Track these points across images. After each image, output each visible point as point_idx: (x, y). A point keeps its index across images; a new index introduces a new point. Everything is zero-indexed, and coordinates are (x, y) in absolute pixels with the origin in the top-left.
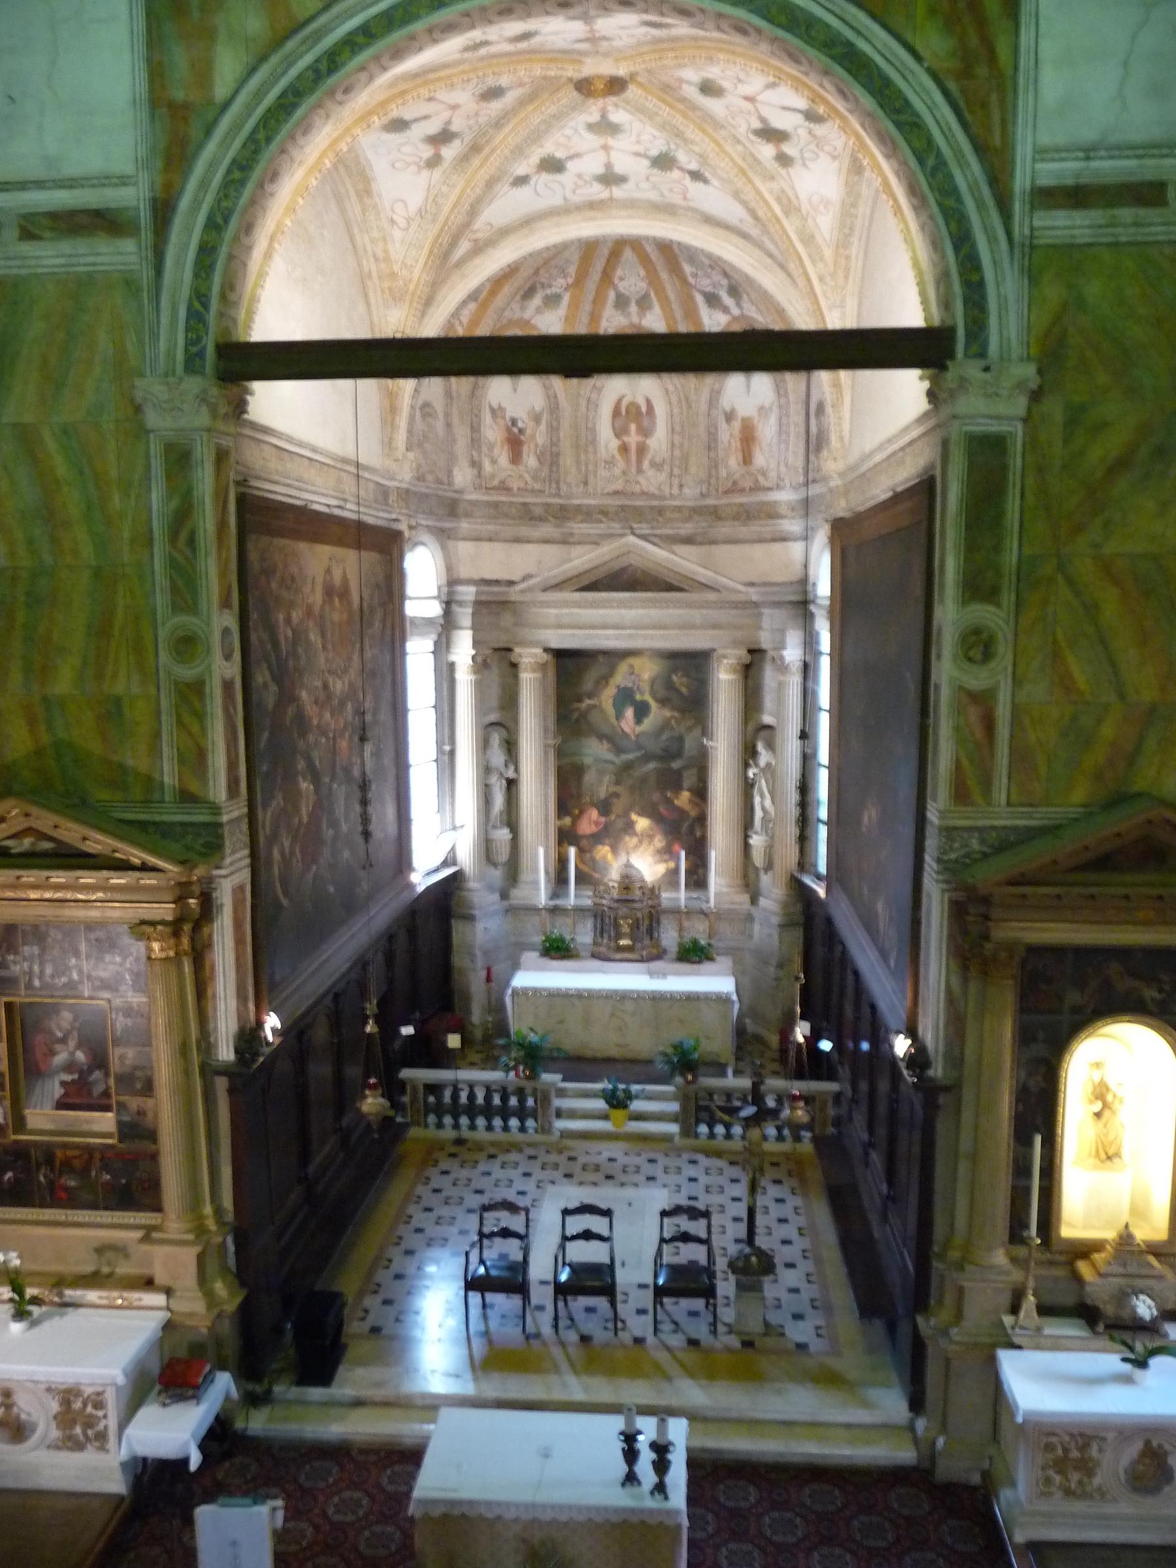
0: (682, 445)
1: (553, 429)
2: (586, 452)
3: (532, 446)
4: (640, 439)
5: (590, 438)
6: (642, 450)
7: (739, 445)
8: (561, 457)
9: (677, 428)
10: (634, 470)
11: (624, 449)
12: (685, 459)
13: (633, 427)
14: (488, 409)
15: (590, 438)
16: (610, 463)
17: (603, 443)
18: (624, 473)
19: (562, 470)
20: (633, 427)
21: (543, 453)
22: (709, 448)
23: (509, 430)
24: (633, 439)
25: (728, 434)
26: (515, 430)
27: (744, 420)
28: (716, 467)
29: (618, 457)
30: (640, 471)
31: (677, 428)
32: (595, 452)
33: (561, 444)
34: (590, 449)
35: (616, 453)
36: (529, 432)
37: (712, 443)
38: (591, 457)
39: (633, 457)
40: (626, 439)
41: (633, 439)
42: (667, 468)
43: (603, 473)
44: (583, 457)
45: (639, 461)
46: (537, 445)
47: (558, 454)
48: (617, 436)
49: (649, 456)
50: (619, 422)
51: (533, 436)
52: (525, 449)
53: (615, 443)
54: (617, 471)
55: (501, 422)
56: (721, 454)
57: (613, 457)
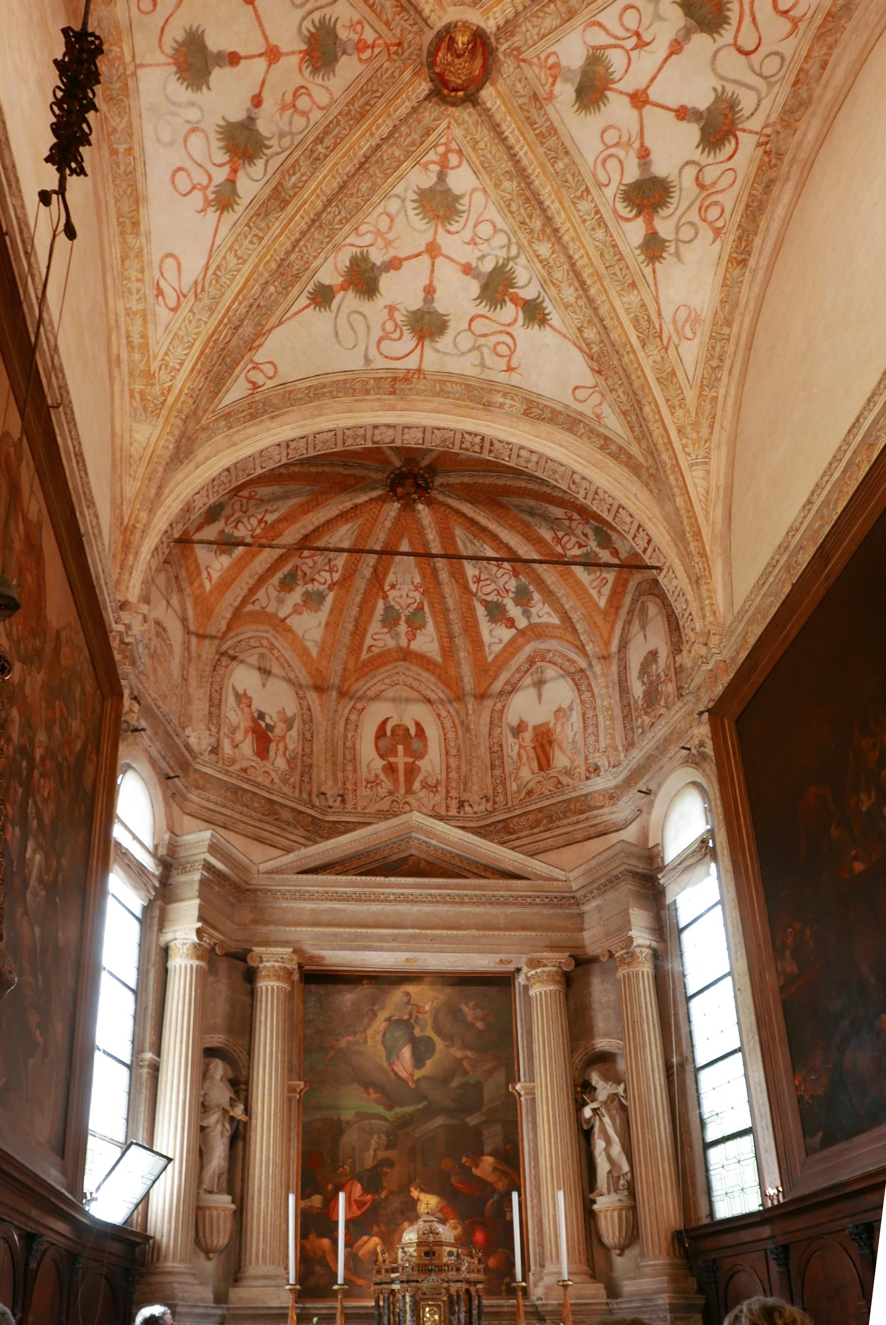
0: (459, 768)
1: (307, 739)
2: (344, 771)
3: (281, 745)
4: (411, 760)
5: (349, 757)
6: (411, 771)
7: (532, 753)
8: (315, 772)
9: (453, 752)
10: (402, 790)
11: (391, 769)
12: (465, 782)
13: (400, 748)
14: (230, 689)
15: (349, 757)
16: (374, 783)
17: (364, 763)
18: (390, 793)
19: (315, 784)
20: (400, 748)
21: (294, 758)
22: (493, 767)
23: (254, 720)
24: (401, 760)
25: (516, 748)
26: (263, 724)
27: (535, 728)
28: (504, 783)
29: (383, 777)
30: (409, 791)
31: (453, 752)
32: (355, 771)
33: (315, 758)
34: (350, 767)
35: (380, 772)
36: (278, 731)
37: (497, 753)
38: (350, 776)
39: (402, 778)
40: (392, 760)
41: (401, 760)
42: (442, 789)
43: (364, 792)
44: (340, 775)
45: (409, 782)
46: (286, 748)
47: (311, 766)
48: (382, 756)
49: (420, 778)
50: (383, 743)
51: (283, 738)
52: (273, 746)
53: (379, 764)
54: (382, 791)
55: (246, 710)
56: (509, 768)
57: (377, 776)
